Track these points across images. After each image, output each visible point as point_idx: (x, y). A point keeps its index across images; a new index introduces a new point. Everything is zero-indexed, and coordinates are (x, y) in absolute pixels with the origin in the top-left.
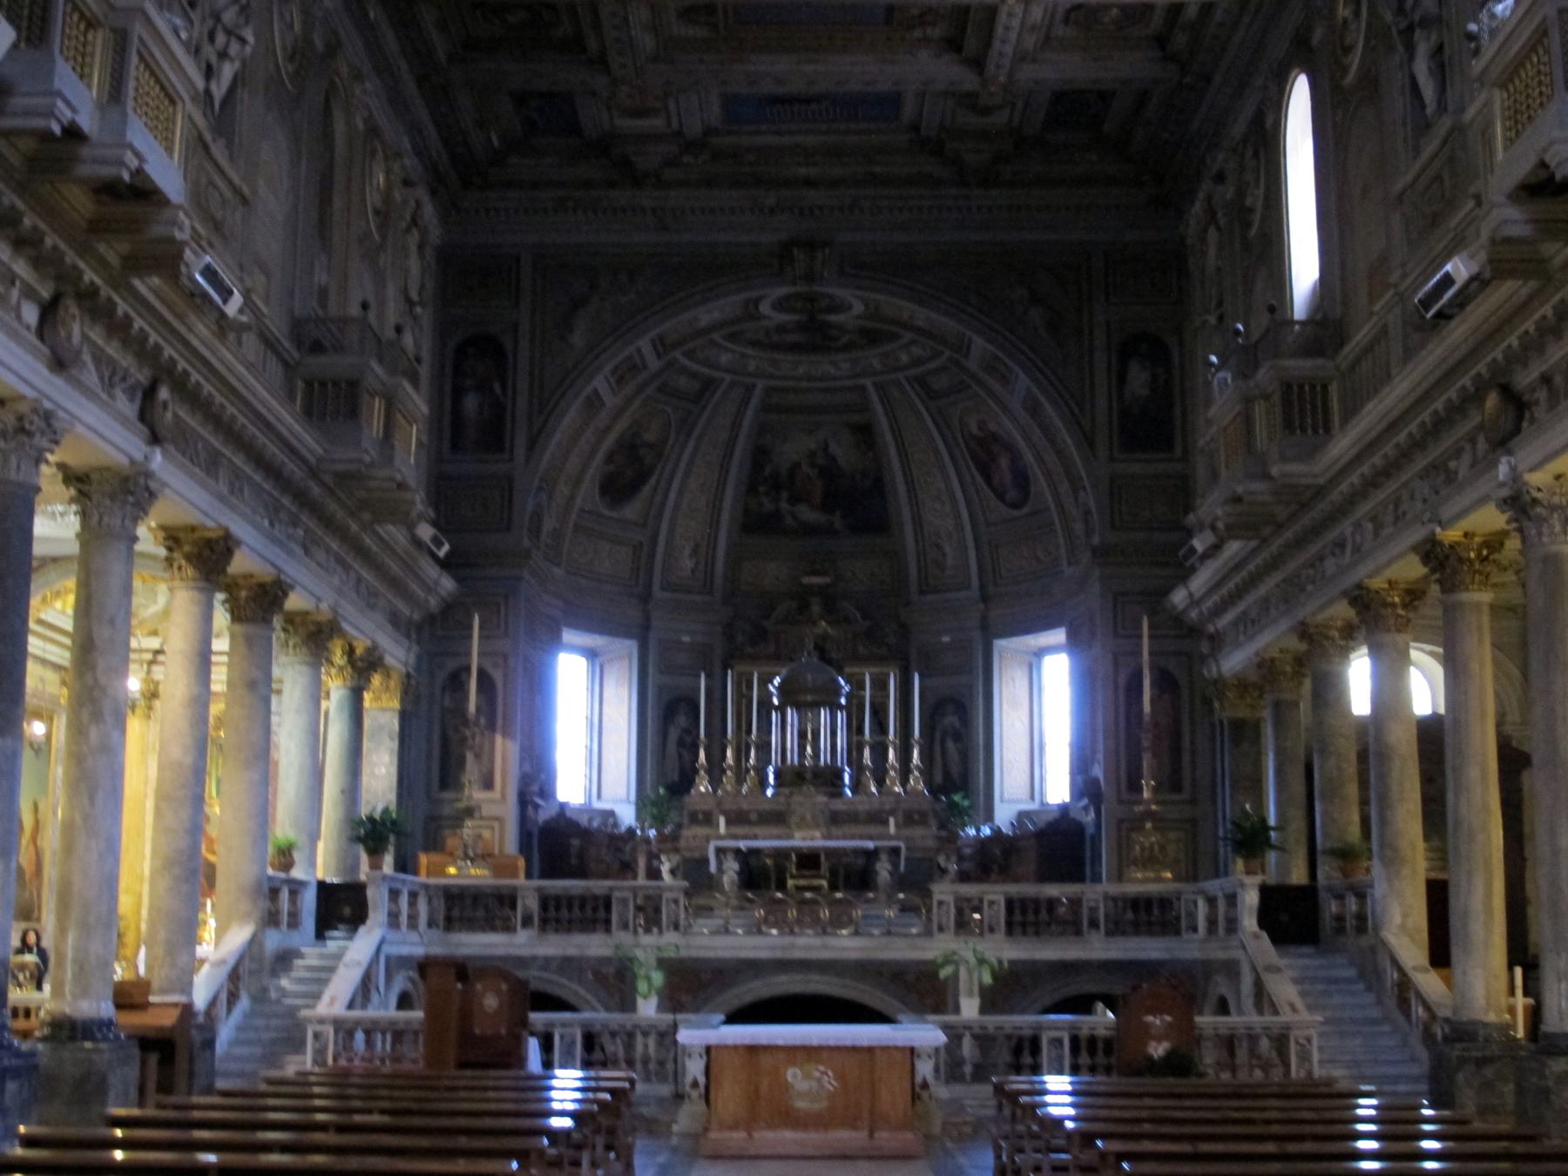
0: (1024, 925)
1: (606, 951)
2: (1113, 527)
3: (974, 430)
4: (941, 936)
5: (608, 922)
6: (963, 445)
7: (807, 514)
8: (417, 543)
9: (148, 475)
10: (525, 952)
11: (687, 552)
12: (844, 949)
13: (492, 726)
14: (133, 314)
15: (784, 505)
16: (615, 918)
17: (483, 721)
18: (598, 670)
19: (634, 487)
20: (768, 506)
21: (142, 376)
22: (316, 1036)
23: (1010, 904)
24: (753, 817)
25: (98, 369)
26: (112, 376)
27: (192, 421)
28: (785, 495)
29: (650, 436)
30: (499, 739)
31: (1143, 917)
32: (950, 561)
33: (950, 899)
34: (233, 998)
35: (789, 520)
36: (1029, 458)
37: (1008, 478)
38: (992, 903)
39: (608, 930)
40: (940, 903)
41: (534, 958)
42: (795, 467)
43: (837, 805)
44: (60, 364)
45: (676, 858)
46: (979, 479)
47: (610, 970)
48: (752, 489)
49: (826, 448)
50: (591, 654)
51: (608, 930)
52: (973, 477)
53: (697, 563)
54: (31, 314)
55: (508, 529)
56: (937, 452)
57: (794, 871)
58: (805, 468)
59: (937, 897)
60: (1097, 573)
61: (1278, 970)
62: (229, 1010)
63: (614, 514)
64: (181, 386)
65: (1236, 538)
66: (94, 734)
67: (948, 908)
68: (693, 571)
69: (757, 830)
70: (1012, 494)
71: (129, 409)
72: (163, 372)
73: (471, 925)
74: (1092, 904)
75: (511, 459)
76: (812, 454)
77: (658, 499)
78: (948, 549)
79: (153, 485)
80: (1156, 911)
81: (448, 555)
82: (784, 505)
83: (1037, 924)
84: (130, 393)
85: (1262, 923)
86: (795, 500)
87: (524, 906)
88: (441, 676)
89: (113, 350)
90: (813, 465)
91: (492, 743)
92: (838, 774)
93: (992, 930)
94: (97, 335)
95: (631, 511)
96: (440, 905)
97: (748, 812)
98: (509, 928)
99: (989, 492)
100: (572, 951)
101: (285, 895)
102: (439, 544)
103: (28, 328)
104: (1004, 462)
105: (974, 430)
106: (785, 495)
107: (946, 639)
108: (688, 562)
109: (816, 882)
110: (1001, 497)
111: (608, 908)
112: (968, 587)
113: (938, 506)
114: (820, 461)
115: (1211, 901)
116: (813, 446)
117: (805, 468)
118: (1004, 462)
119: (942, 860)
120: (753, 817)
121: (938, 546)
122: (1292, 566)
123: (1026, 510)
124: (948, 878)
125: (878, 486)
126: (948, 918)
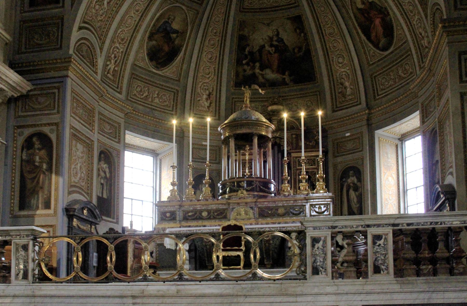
0: (417, 262)
2: (456, 8)
3: (360, 6)
6: (353, 17)
7: (271, 75)
11: (205, 97)
13: (50, 169)
15: (257, 71)
17: (45, 166)
18: (158, 162)
20: (249, 72)
24: (205, 214)
28: (257, 64)
30: (54, 176)
32: (349, 91)
35: (260, 77)
37: (380, 30)
40: (315, 241)
42: (263, 47)
43: (264, 203)
46: (363, 37)
48: (239, 62)
49: (278, 34)
50: (154, 153)
52: (360, 38)
53: (211, 103)
55: (61, 48)
56: (339, 26)
57: (222, 248)
58: (267, 48)
60: (446, 40)
63: (160, 73)
67: (324, 246)
68: (209, 107)
69: (206, 223)
70: (383, 41)
75: (63, 6)
76: (271, 39)
77: (185, 67)
78: (347, 84)
82: (257, 71)
83: (433, 261)
88: (21, 140)
90: (271, 46)
91: (50, 179)
92: (266, 184)
93: (377, 270)
95: (169, 71)
97: (201, 211)
99: (370, 45)
104: (377, 21)
106: (257, 64)
107: (348, 134)
108: (206, 103)
112: (360, 104)
113: (341, 60)
114: (275, 43)
116: (270, 34)
117: (267, 48)
118: (377, 21)
120: (205, 214)
121: (342, 84)
125: (308, 53)
126: (325, 259)
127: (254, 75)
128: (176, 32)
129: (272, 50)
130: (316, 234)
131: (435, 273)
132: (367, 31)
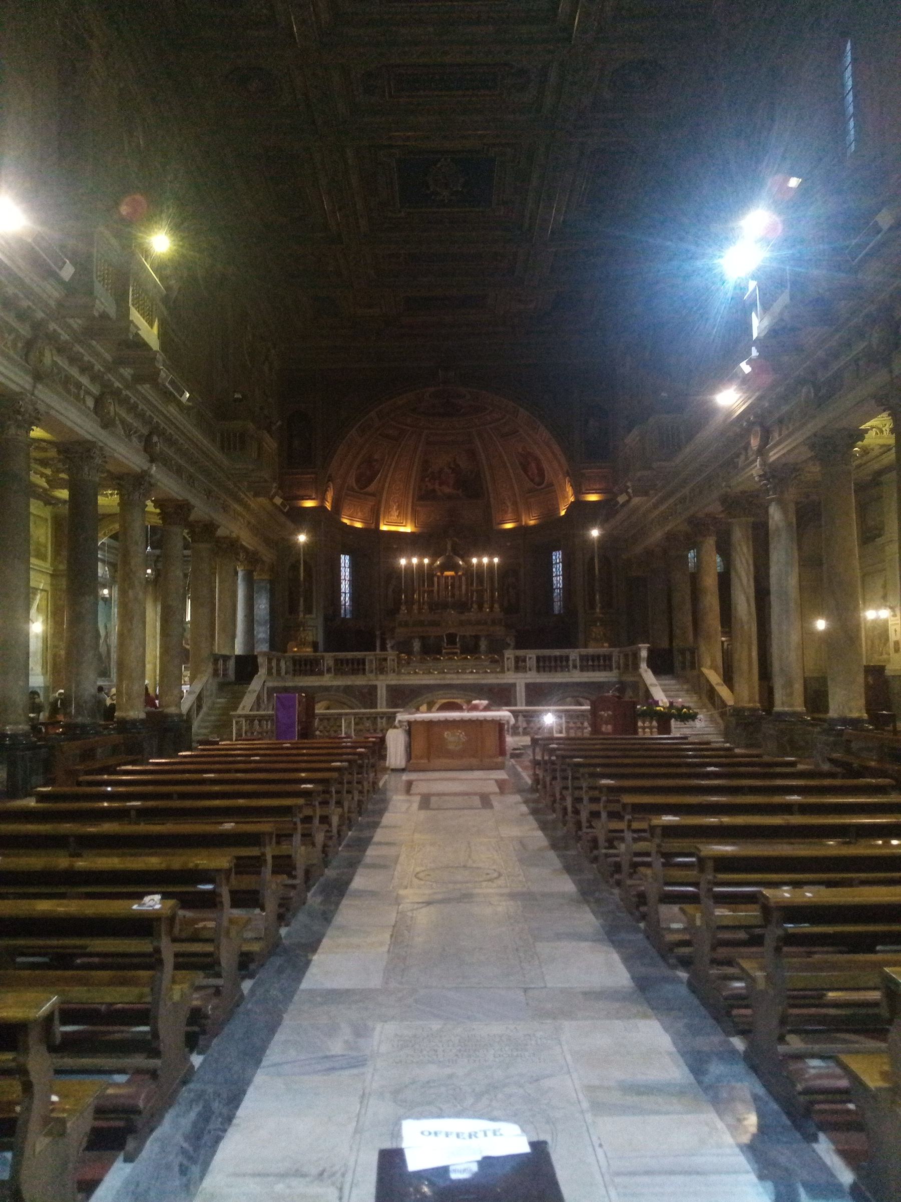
0: (544, 667)
1: (364, 683)
3: (520, 450)
4: (508, 673)
5: (364, 670)
7: (447, 490)
8: (274, 505)
9: (151, 476)
10: (330, 684)
12: (468, 679)
14: (139, 402)
15: (437, 487)
16: (367, 667)
19: (370, 480)
21: (145, 431)
22: (237, 723)
23: (538, 658)
25: (124, 428)
26: (129, 431)
27: (170, 452)
28: (437, 482)
29: (376, 457)
31: (596, 663)
33: (512, 656)
34: (199, 707)
36: (545, 465)
37: (536, 471)
38: (530, 658)
39: (364, 673)
40: (508, 659)
41: (332, 686)
44: (107, 424)
45: (393, 642)
47: (366, 690)
49: (455, 460)
51: (364, 673)
54: (90, 403)
59: (506, 656)
61: (656, 685)
62: (198, 714)
64: (162, 434)
65: (638, 496)
66: (131, 593)
70: (537, 479)
71: (140, 446)
72: (155, 430)
73: (305, 673)
74: (574, 658)
79: (153, 481)
80: (602, 661)
81: (288, 512)
82: (437, 487)
84: (140, 437)
85: (648, 666)
86: (440, 485)
87: (327, 664)
89: (129, 419)
90: (450, 468)
93: (530, 670)
94: (123, 413)
96: (290, 664)
98: (321, 673)
100: (349, 683)
101: (221, 662)
102: (285, 506)
103: (89, 408)
104: (533, 465)
105: (520, 450)
106: (437, 482)
109: (455, 650)
110: (532, 480)
111: (364, 664)
115: (626, 656)
118: (533, 465)
119: (508, 640)
122: (662, 508)
123: (543, 486)
124: (512, 647)
127: (434, 491)
128: (377, 460)
129: (450, 471)
130: (509, 656)
131: (550, 671)
132: (526, 471)
